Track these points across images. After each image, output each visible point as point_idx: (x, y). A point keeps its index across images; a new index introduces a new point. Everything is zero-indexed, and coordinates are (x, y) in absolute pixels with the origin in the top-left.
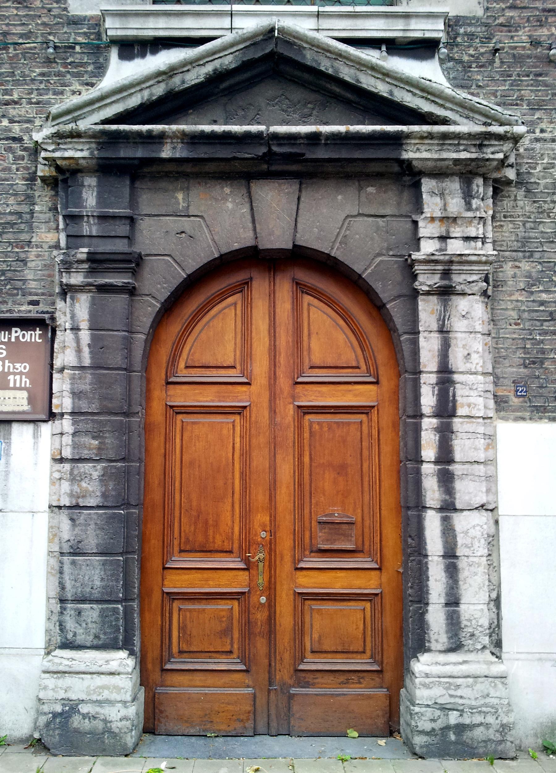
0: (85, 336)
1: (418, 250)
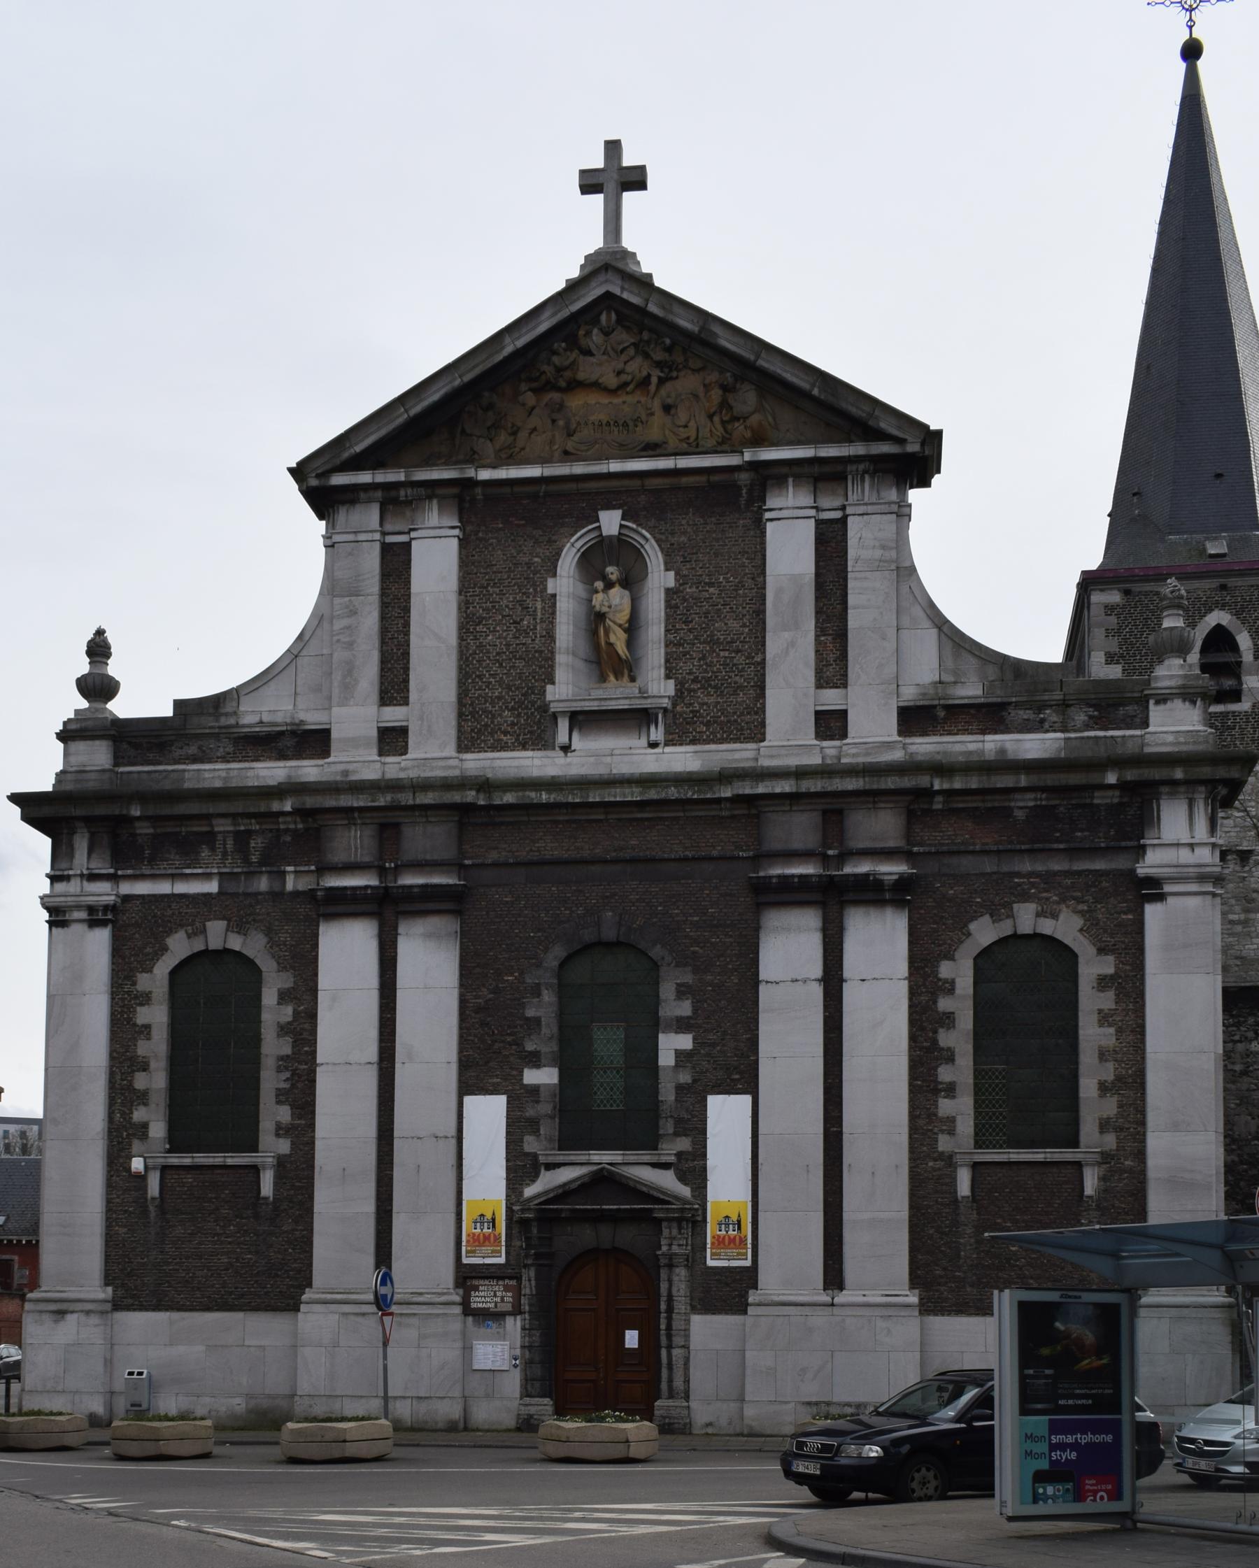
0: (533, 1283)
1: (660, 1249)
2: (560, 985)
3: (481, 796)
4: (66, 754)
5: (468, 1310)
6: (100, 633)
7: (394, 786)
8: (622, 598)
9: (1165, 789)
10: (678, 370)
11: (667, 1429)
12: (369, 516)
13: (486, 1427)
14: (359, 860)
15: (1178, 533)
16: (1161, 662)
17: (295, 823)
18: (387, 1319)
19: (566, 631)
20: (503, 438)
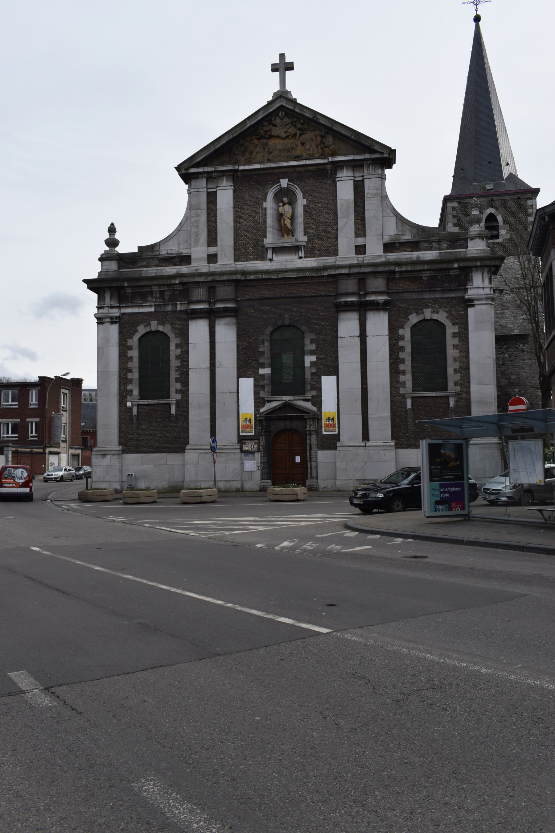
0: (264, 441)
2: (271, 340)
3: (243, 277)
4: (102, 266)
5: (242, 451)
6: (112, 224)
7: (213, 274)
8: (289, 208)
9: (473, 269)
10: (306, 131)
11: (310, 489)
12: (202, 183)
13: (249, 490)
14: (202, 299)
15: (476, 182)
16: (471, 226)
17: (180, 287)
18: (215, 455)
19: (270, 220)
20: (247, 155)
